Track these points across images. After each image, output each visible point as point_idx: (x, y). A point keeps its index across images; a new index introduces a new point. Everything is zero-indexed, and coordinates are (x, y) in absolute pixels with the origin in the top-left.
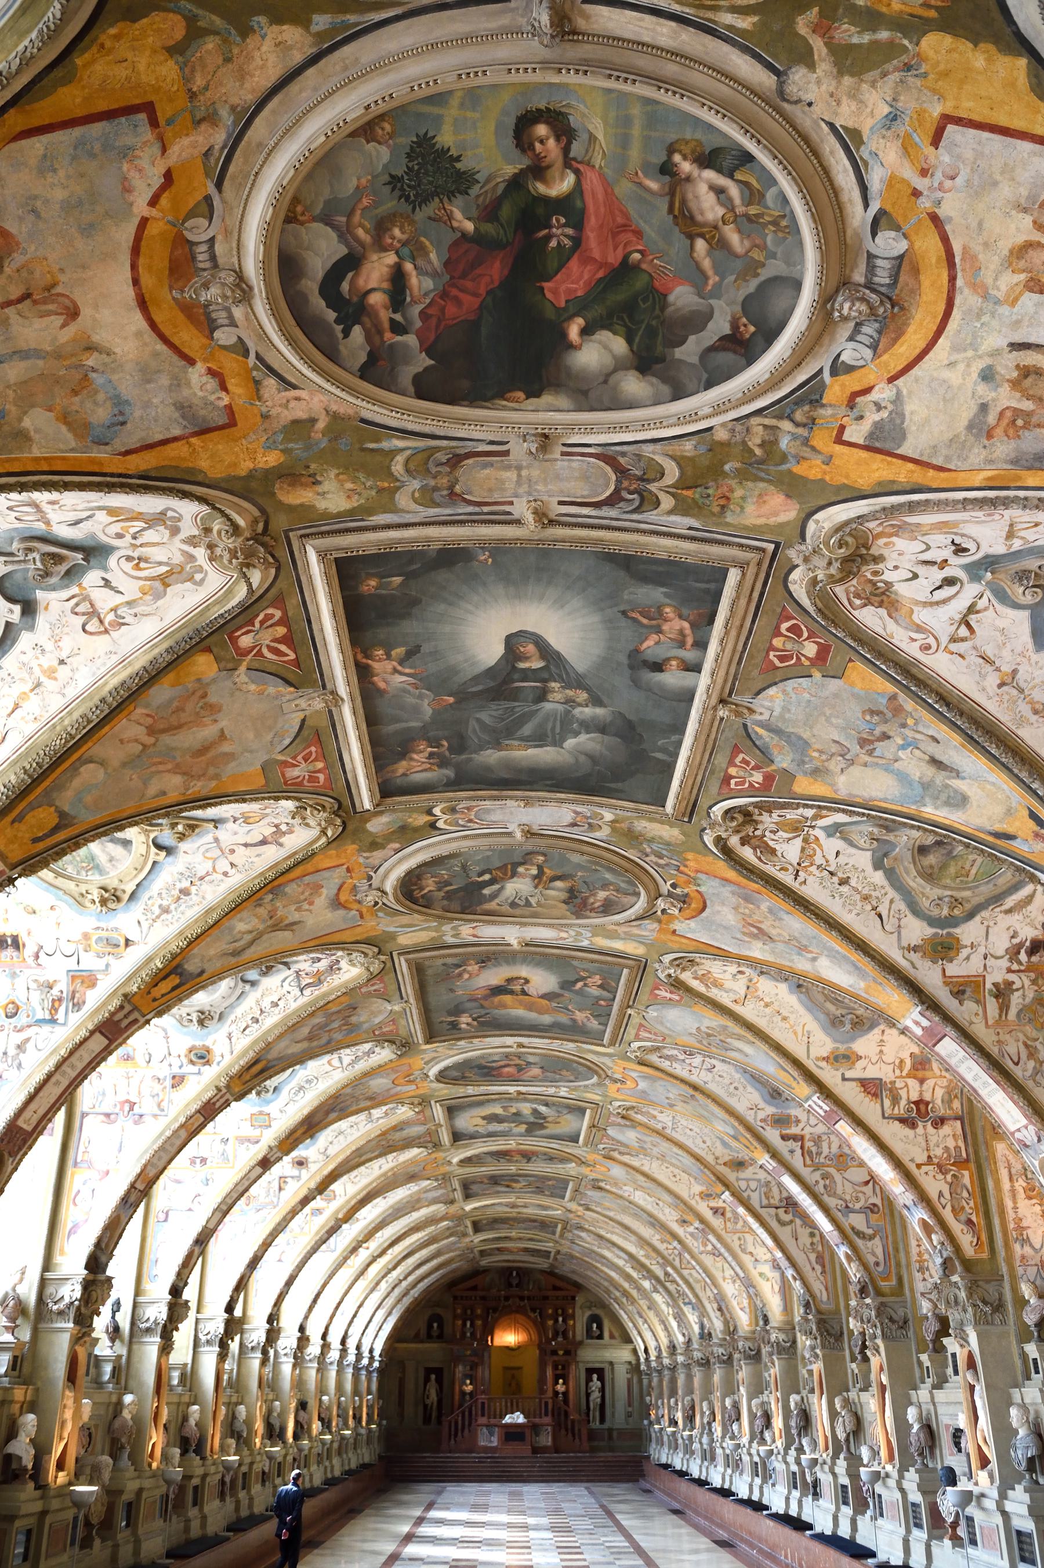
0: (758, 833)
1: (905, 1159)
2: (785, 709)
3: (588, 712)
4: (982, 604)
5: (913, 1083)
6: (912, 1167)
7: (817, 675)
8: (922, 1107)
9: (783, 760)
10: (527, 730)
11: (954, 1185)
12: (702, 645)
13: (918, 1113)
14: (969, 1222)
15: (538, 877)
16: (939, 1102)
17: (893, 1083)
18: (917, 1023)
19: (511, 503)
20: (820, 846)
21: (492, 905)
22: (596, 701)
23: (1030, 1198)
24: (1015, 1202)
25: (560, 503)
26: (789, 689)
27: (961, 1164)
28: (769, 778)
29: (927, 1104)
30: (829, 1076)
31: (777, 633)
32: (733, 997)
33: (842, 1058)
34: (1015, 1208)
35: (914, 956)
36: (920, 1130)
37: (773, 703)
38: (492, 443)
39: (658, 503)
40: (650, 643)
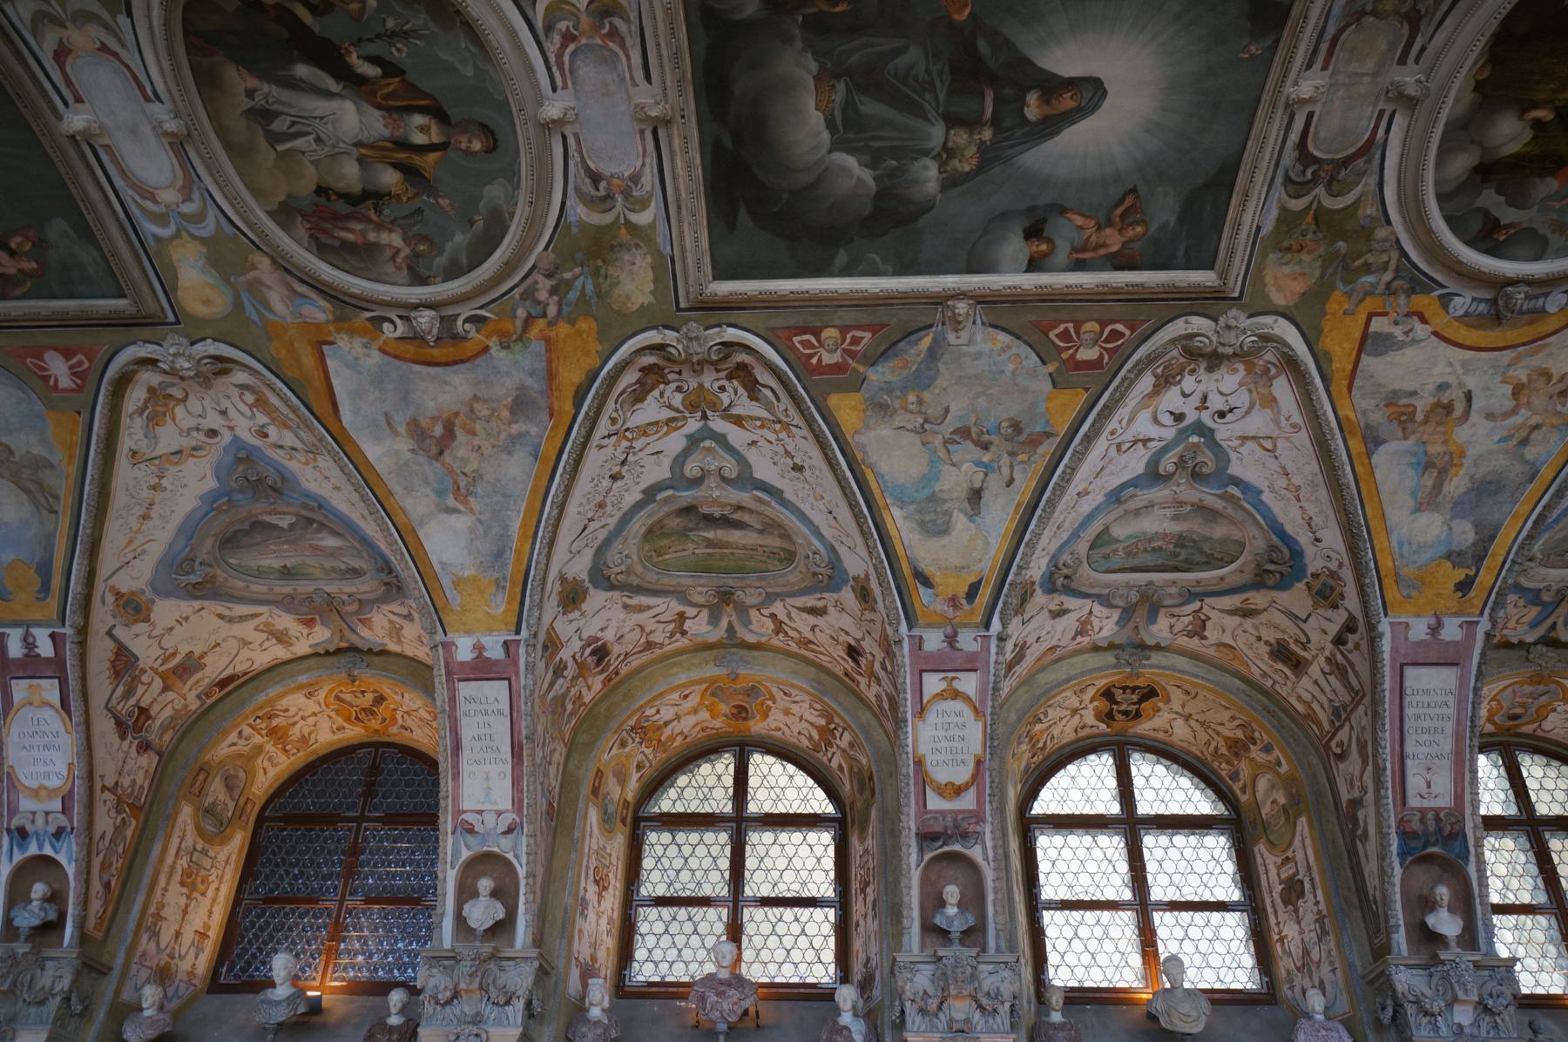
0: (671, 377)
1: (98, 771)
2: (977, 356)
3: (929, 176)
4: (1151, 444)
5: (158, 683)
6: (98, 785)
7: (1051, 368)
8: (142, 719)
9: (877, 375)
10: (870, 107)
11: (119, 829)
12: (1079, 266)
13: (133, 724)
14: (107, 886)
15: (403, 145)
16: (158, 722)
17: (143, 671)
18: (479, 648)
19: (1324, 68)
20: (666, 434)
21: (237, 80)
22: (951, 182)
23: (183, 884)
24: (168, 883)
25: (1311, 115)
26: (1014, 351)
27: (136, 809)
28: (838, 368)
29: (149, 718)
30: (102, 616)
31: (1103, 325)
32: (143, 445)
33: (133, 608)
34: (165, 890)
35: (558, 583)
36: (126, 744)
37: (984, 347)
38: (1423, 49)
39: (1296, 197)
40: (1079, 220)
